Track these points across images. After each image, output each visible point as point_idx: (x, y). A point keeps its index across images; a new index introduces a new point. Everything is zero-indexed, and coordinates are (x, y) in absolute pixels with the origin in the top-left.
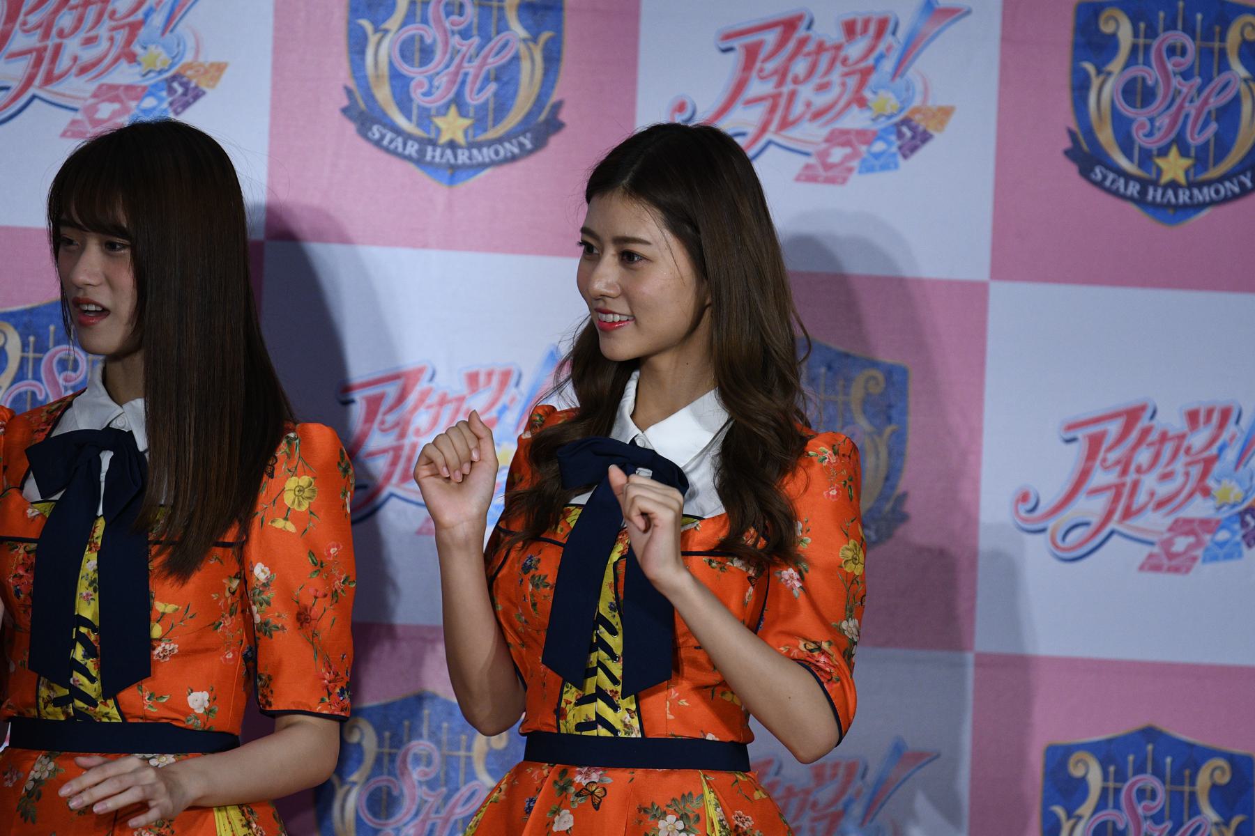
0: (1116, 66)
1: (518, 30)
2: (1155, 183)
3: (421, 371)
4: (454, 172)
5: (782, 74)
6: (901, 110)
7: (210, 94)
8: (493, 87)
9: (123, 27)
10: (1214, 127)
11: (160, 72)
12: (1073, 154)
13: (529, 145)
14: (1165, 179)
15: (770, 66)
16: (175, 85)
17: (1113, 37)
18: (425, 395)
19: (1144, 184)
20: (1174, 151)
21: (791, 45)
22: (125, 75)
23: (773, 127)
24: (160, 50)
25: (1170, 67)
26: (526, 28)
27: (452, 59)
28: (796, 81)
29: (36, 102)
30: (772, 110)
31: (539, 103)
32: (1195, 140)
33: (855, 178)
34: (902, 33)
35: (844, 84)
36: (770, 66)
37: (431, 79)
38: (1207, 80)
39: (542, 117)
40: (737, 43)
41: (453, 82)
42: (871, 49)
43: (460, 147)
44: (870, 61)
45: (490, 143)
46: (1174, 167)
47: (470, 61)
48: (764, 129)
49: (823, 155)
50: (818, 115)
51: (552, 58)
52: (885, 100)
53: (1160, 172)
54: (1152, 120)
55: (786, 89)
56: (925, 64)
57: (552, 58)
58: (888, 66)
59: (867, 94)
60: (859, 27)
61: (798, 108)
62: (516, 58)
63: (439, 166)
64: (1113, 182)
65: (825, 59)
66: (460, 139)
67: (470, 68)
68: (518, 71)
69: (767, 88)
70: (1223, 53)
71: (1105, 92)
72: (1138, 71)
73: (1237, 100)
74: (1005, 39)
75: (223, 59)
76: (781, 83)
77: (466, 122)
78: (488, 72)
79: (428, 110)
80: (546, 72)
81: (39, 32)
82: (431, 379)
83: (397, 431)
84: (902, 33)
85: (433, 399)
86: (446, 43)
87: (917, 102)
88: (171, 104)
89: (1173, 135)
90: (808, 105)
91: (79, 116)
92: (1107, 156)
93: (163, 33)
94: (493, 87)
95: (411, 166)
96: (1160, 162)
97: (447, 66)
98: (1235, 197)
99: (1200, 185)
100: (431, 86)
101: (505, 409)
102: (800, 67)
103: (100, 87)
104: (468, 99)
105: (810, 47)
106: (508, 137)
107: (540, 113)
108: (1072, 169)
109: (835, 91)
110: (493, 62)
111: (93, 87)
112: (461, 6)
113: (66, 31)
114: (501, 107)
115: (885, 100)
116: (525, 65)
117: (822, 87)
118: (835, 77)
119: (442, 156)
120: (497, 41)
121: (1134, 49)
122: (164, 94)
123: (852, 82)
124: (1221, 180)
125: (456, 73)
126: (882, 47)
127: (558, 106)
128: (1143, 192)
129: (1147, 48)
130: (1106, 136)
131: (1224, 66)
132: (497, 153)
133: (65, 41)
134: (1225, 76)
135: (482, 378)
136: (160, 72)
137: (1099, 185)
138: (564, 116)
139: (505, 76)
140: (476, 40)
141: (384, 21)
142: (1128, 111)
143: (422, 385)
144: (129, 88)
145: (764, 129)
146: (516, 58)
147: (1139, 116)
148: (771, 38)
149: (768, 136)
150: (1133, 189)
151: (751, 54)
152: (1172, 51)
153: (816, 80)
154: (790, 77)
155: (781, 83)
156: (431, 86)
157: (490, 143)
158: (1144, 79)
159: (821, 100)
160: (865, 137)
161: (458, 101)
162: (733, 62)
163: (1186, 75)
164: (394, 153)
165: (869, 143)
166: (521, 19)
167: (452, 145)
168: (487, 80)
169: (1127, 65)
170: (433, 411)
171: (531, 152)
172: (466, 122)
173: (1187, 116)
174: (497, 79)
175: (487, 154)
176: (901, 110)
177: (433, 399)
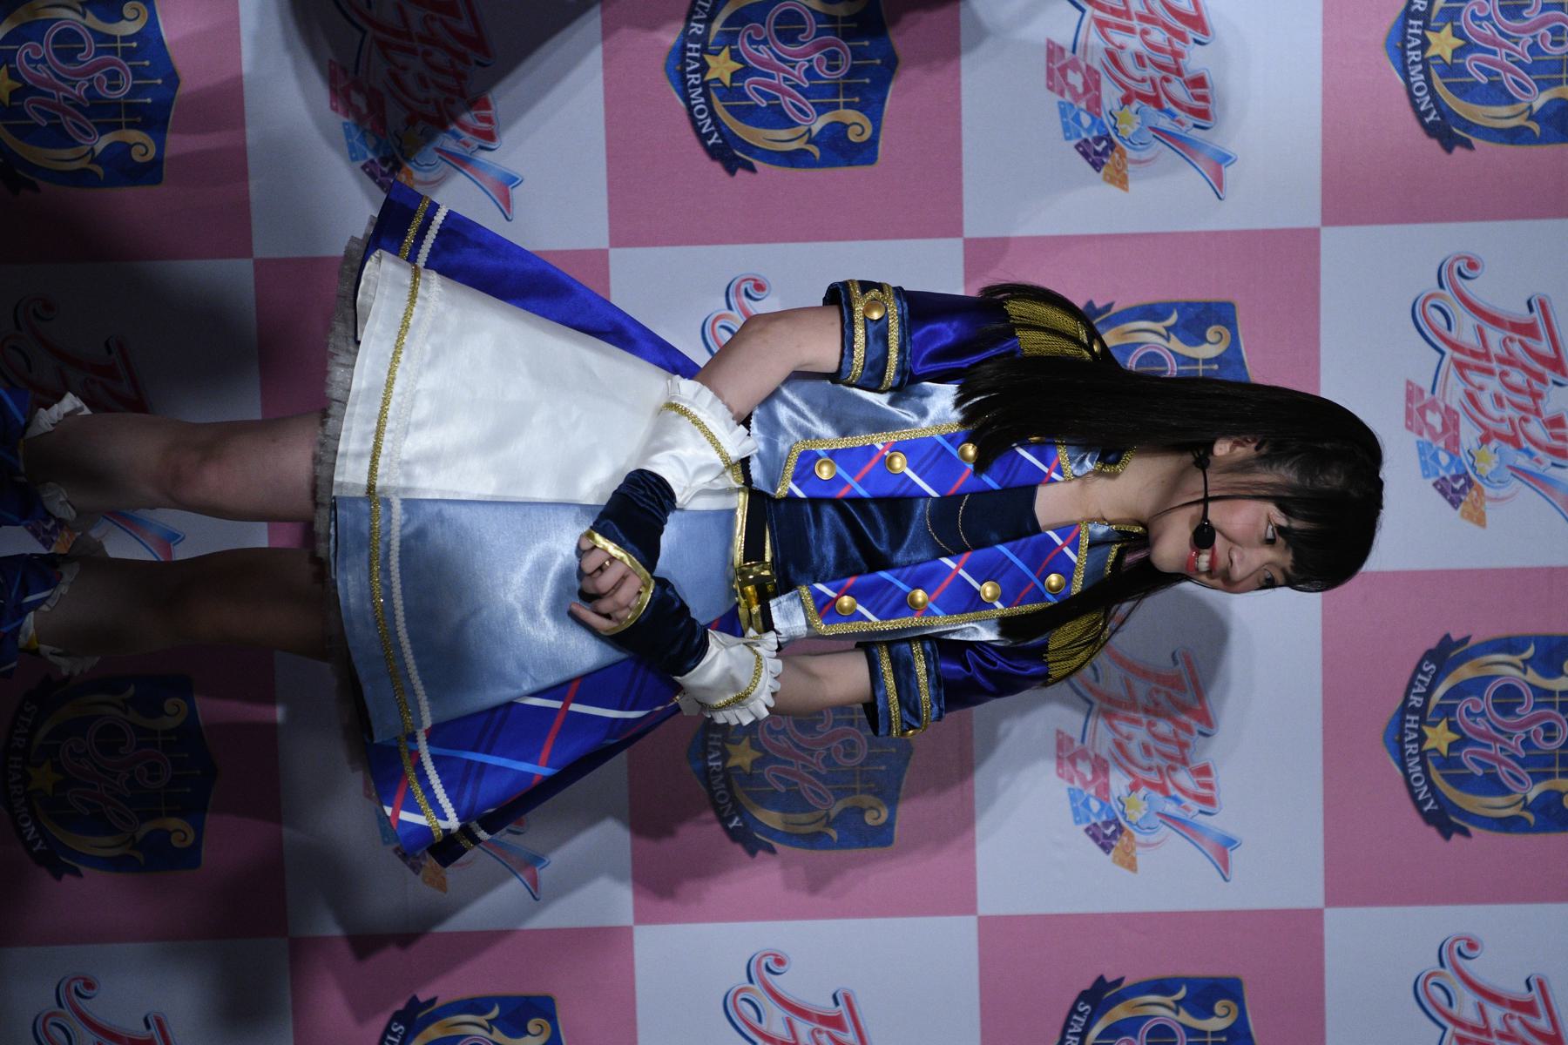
0: (1532, 676)
1: (1540, 100)
2: (1422, 721)
3: (1205, 32)
4: (1398, 48)
5: (1509, 361)
6: (1480, 477)
7: (1454, 515)
8: (1484, 80)
9: (1514, 429)
10: (1479, 772)
11: (1473, 466)
12: (1446, 643)
13: (1427, 120)
14: (1427, 730)
15: (1516, 348)
16: (1462, 481)
17: (1561, 673)
18: (1188, 729)
19: (1421, 712)
20: (1454, 737)
21: (1538, 367)
22: (1469, 434)
23: (1458, 355)
24: (1494, 466)
25: (1534, 727)
26: (1542, 109)
27: (1507, 37)
28: (1503, 374)
29: (1438, 356)
30: (1474, 354)
31: (1469, 126)
32: (1465, 755)
33: (1413, 438)
34: (1555, 473)
35: (1502, 420)
36: (1516, 348)
37: (1489, 18)
38: (1523, 763)
39: (1453, 819)
40: (1537, 314)
41: (1486, 39)
42: (1536, 444)
43: (1421, 746)
44: (1526, 444)
45: (1428, 80)
46: (1439, 738)
47: (1508, 55)
48: (1456, 347)
49: (1433, 405)
50: (1471, 397)
51: (1515, 136)
52: (1489, 461)
53: (1434, 725)
54: (1483, 714)
55: (1495, 365)
56: (1526, 495)
57: (1515, 136)
58: (1522, 461)
59: (1494, 444)
60: (1558, 431)
61: (1477, 378)
62: (1512, 100)
63: (1405, 34)
64: (1422, 682)
65: (1526, 401)
66: (1430, 53)
67: (1501, 55)
68: (1498, 104)
69: (1495, 347)
70: (1549, 776)
71: (1506, 668)
72: (1529, 697)
73: (1506, 791)
74: (1551, 572)
75: (1488, 523)
76: (1501, 360)
77: (1448, 57)
78: (1498, 74)
79: (1453, 714)
80: (1501, 131)
81: (1505, 354)
82: (1196, 41)
83: (1151, 705)
84: (1555, 473)
85: (1183, 736)
86: (1524, 32)
87: (1489, 491)
88: (1444, 479)
89: (1469, 735)
90: (1481, 388)
91: (1427, 395)
92: (1446, 675)
93: (1510, 467)
94: (1484, 80)
95: (1403, 6)
96: (1443, 724)
97: (1502, 34)
98: (1414, 796)
99: (1423, 763)
100: (1481, 19)
101: (1172, 115)
102: (1517, 377)
103: (1456, 413)
104: (1469, 57)
105: (1536, 385)
106: (1432, 787)
107: (1458, 817)
108: (1432, 643)
109: (1496, 413)
110: (1507, 79)
111: (1456, 407)
112: (1561, 43)
113: (1507, 379)
114: (1466, 90)
115: (1489, 461)
116: (1505, 110)
117: (1498, 401)
118: (1509, 412)
119: (1413, 35)
120: (1529, 81)
121: (1551, 693)
122: (1453, 471)
123: (1505, 429)
124: (1429, 782)
125: (1495, 43)
126: (1540, 454)
127: (1468, 145)
128: (1414, 710)
129: (1551, 705)
130: (1465, 672)
131: (1537, 778)
132: (1417, 779)
133: (1497, 378)
134: (1528, 779)
135: (1199, 91)
136: (1473, 466)
137: (1418, 669)
138: (1455, 837)
139: (1497, 93)
140: (1522, 754)
141: (1533, 667)
142: (1490, 690)
143: (1196, 726)
144: (1456, 441)
145: (1456, 347)
146: (1512, 100)
147: (1486, 702)
148: (1544, 347)
149: (1450, 1027)
150: (1416, 701)
151: (1529, 330)
152: (1550, 728)
153: (1504, 393)
154: (1506, 368)
155: (1501, 360)
156: (1481, 19)
157: (1428, 80)
158: (1521, 704)
159: (1486, 400)
160: (1453, 444)
161: (1462, 742)
162: (1519, 312)
163: (1527, 743)
164: (1411, 685)
165: (1447, 449)
166: (1550, 102)
167: (1425, 44)
168: (1488, 73)
169: (1532, 687)
170: (1166, 45)
171: (1420, 811)
172: (1448, 57)
173: (1489, 747)
174: (1490, 82)
175: (1418, 79)
176: (1480, 477)
177: (1183, 736)
